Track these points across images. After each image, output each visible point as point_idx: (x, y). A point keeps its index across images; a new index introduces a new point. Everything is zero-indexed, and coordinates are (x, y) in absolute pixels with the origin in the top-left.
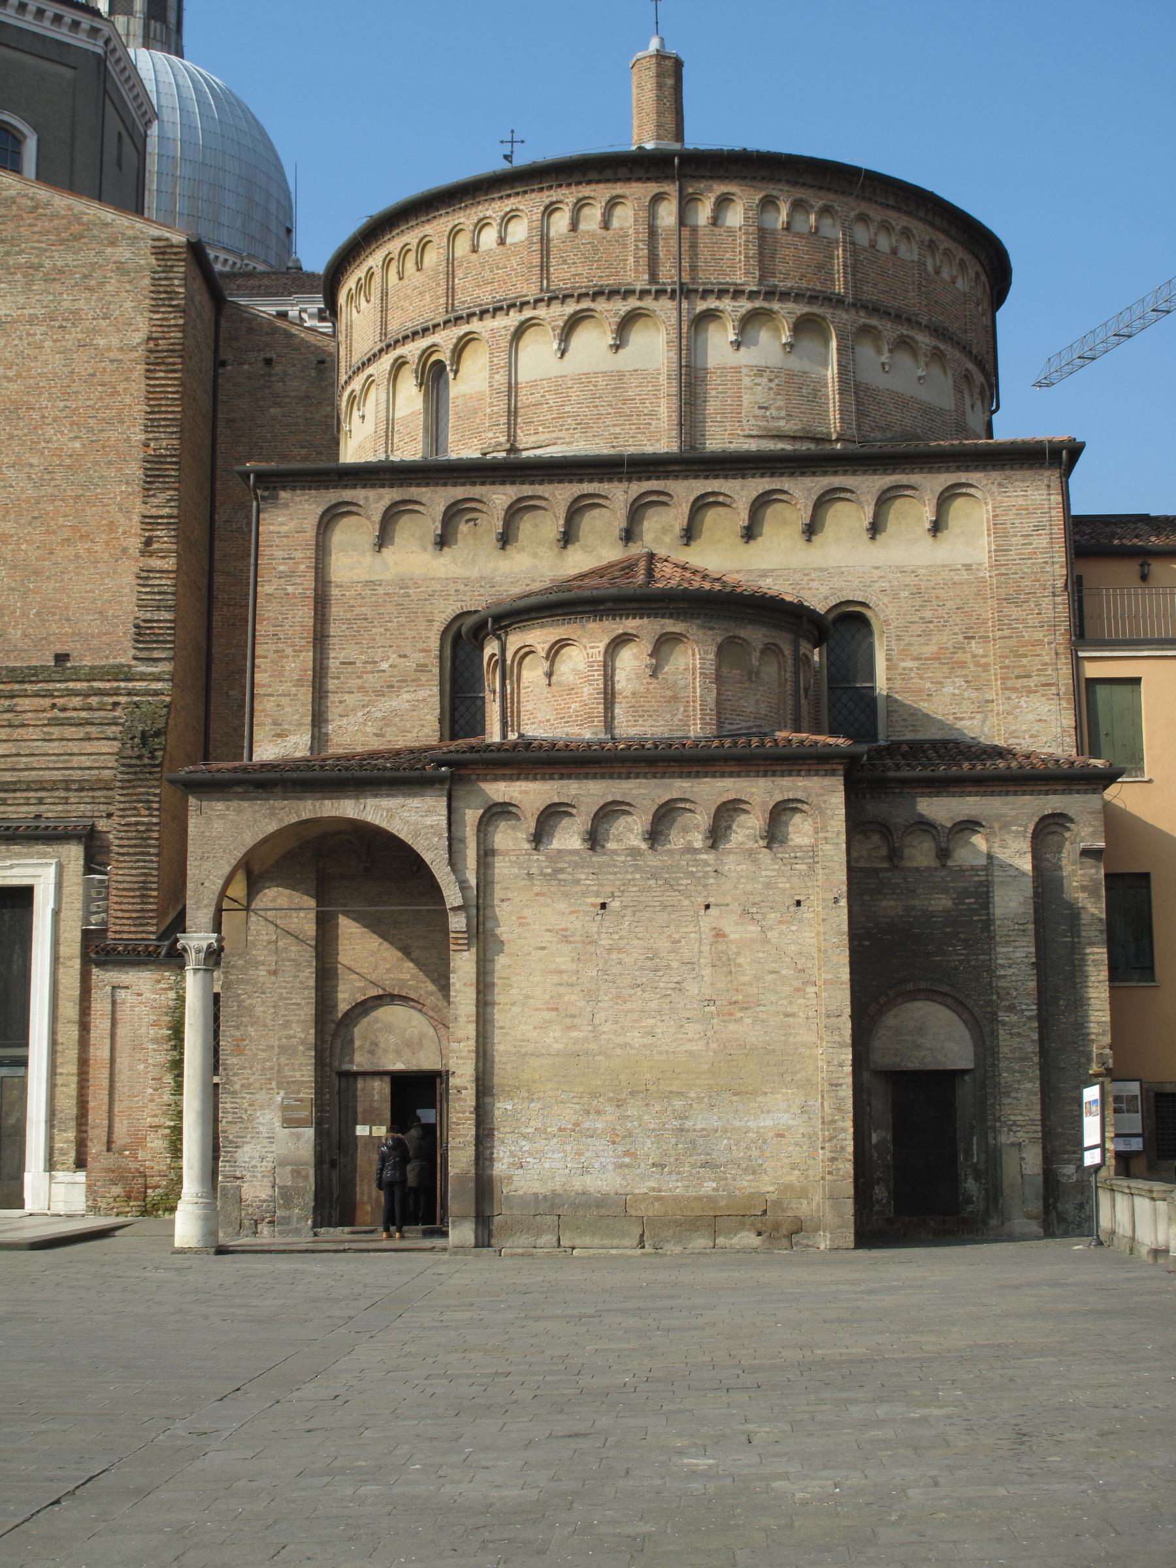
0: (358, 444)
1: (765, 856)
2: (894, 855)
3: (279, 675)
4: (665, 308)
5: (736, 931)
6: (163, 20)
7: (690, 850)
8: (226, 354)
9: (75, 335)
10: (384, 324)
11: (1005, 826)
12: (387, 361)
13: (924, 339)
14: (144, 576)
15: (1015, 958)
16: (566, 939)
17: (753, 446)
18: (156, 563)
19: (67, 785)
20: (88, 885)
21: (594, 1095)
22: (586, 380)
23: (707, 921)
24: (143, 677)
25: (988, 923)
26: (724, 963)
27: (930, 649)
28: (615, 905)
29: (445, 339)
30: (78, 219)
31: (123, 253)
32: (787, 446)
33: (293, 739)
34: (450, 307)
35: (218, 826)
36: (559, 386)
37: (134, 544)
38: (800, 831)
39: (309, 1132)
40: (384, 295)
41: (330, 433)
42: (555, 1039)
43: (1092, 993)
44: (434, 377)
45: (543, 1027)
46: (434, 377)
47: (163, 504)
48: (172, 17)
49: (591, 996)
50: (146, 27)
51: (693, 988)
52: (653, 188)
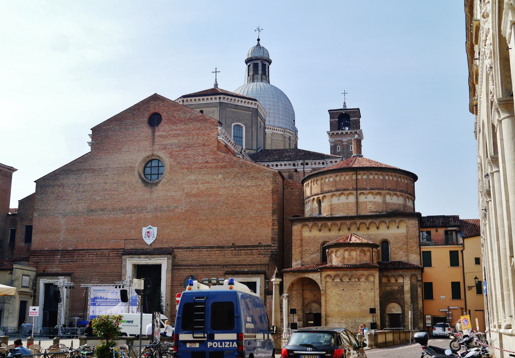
0: (307, 215)
1: (367, 282)
2: (389, 281)
3: (296, 252)
4: (354, 192)
5: (362, 293)
6: (265, 75)
7: (356, 281)
8: (285, 188)
9: (260, 188)
10: (311, 192)
11: (406, 276)
12: (312, 198)
13: (398, 193)
14: (273, 229)
15: (407, 296)
16: (338, 294)
17: (369, 214)
18: (274, 227)
19: (261, 265)
20: (265, 281)
21: (343, 317)
22: (343, 204)
23: (358, 292)
24: (273, 246)
25: (403, 291)
26: (361, 298)
27: (397, 247)
28: (345, 289)
29: (321, 196)
30: (260, 168)
31: (268, 174)
32: (374, 214)
33: (298, 262)
34: (321, 191)
35: (288, 278)
36: (338, 205)
37: (271, 224)
38: (371, 279)
39: (302, 322)
40: (311, 187)
41: (303, 211)
42: (337, 309)
43: (419, 302)
44: (319, 202)
45: (335, 307)
46: (319, 202)
47: (275, 217)
48: (267, 74)
49: (342, 302)
50: (262, 77)
51: (356, 302)
52: (352, 173)
